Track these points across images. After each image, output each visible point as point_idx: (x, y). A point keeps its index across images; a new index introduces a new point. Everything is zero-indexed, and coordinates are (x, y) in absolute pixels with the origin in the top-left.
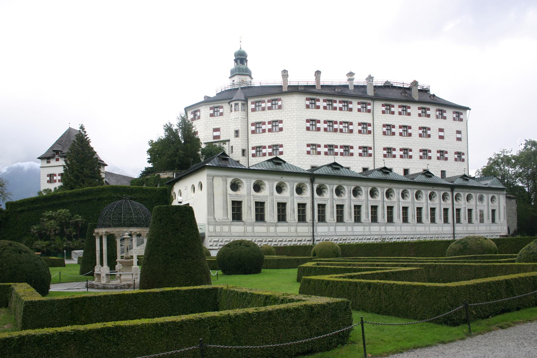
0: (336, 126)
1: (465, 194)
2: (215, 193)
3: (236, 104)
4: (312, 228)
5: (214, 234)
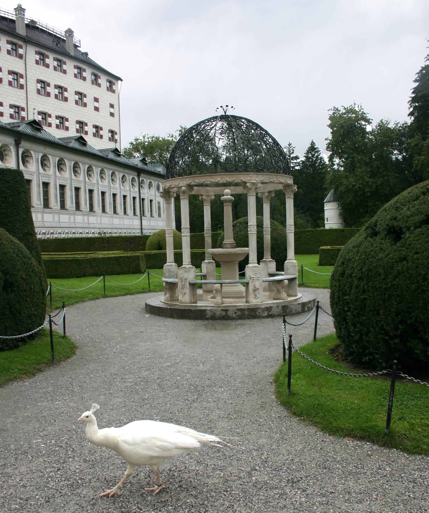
1: (147, 181)
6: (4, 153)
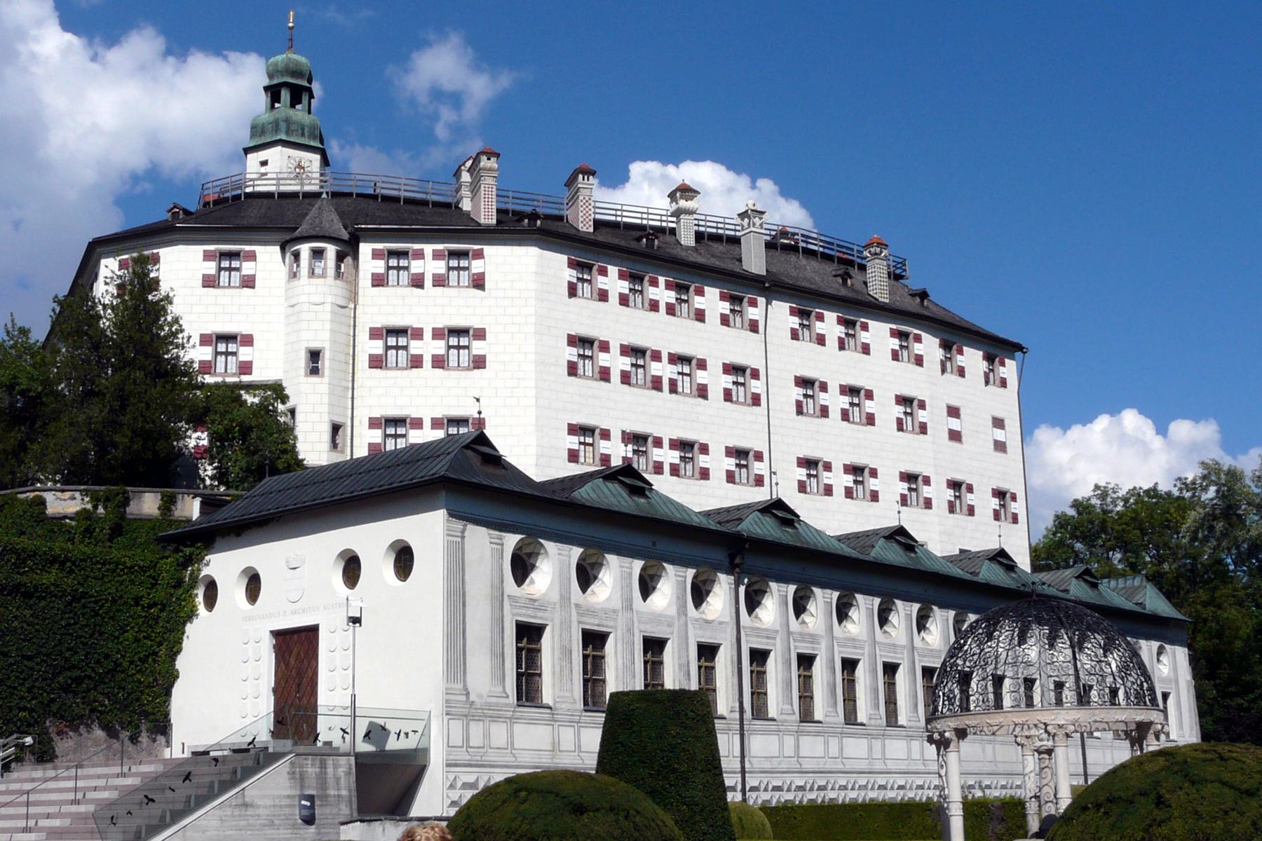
0: (656, 368)
2: (467, 588)
3: (318, 254)
4: (737, 738)
5: (463, 756)
6: (703, 588)
